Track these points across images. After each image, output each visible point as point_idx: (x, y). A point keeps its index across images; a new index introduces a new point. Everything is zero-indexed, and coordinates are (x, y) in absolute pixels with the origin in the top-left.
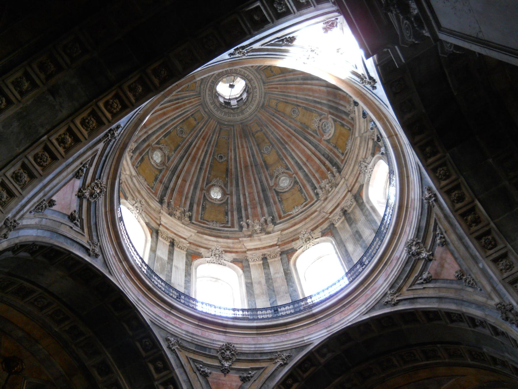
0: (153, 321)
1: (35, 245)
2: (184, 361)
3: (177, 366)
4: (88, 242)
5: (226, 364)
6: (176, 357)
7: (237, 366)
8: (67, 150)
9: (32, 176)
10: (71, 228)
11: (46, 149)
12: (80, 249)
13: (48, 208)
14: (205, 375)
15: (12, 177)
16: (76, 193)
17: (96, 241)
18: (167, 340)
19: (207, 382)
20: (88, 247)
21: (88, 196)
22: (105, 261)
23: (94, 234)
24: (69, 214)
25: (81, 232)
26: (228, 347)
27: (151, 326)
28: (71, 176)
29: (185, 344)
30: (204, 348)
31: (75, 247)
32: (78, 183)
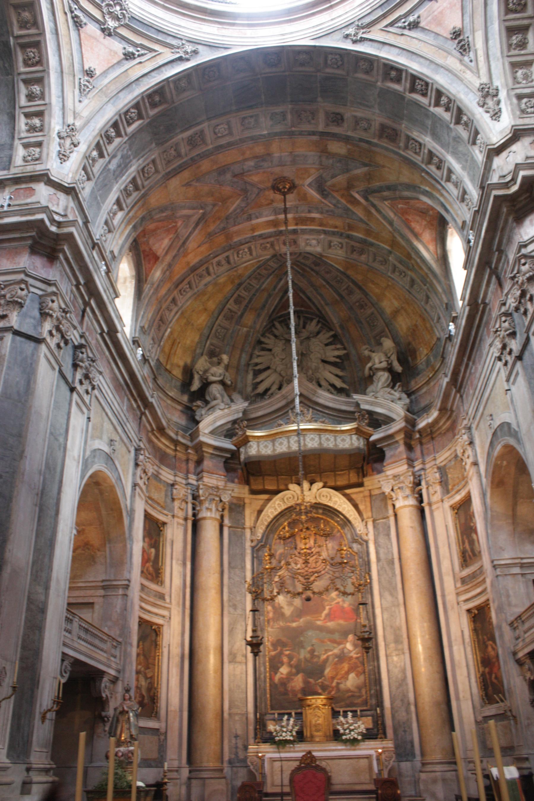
0: (315, 37)
1: (126, 113)
3: (378, 49)
4: (173, 53)
6: (370, 43)
9: (40, 81)
10: (140, 63)
11: (24, 47)
12: (173, 67)
13: (91, 80)
15: (29, 101)
16: (103, 36)
17: (180, 42)
20: (178, 56)
21: (116, 24)
22: (210, 46)
23: (169, 40)
24: (123, 56)
25: (154, 54)
27: (317, 44)
28: (73, 34)
31: (166, 71)
32: (92, 28)
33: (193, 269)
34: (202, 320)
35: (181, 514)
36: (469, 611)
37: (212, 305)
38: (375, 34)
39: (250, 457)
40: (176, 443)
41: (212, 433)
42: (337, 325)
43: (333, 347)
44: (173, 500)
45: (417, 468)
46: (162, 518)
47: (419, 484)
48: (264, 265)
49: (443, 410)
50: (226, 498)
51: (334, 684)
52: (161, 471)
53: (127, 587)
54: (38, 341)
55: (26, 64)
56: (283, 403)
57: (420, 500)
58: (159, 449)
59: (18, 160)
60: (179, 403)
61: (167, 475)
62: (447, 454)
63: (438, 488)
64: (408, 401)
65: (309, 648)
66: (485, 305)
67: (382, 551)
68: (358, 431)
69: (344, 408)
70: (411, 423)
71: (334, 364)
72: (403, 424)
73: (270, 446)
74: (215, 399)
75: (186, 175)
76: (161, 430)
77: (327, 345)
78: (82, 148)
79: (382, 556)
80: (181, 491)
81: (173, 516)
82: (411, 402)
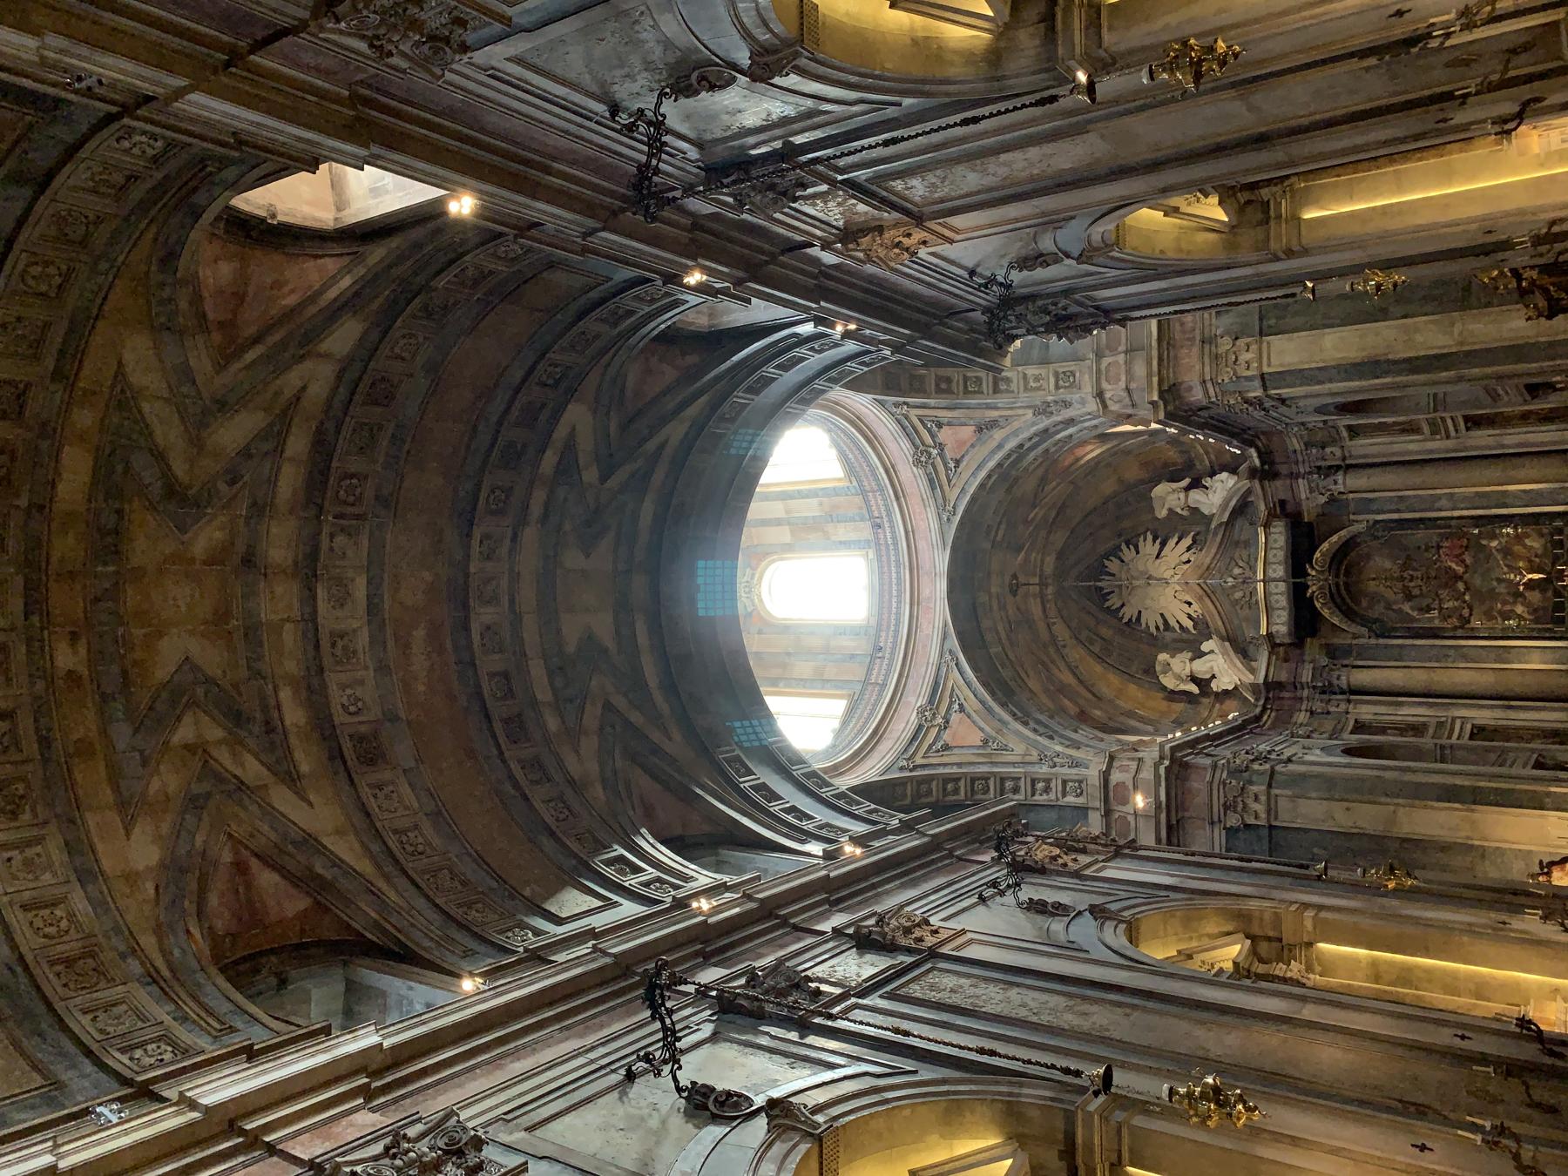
2: (957, 491)
5: (935, 452)
7: (929, 440)
8: (955, 779)
9: (1003, 780)
14: (957, 462)
18: (948, 519)
19: (963, 456)
26: (917, 463)
28: (956, 751)
29: (940, 501)
30: (931, 481)
32: (947, 736)
33: (1081, 682)
34: (1114, 679)
35: (1343, 706)
36: (1468, 429)
37: (1099, 669)
38: (952, 495)
39: (1290, 634)
40: (1264, 709)
41: (1253, 671)
42: (1117, 542)
43: (1141, 544)
44: (1328, 713)
45: (1302, 470)
46: (1352, 723)
47: (1319, 468)
48: (1059, 611)
49: (1251, 444)
50: (1324, 661)
51: (1537, 560)
52: (1299, 721)
53: (1442, 747)
54: (1273, 772)
55: (986, 791)
56: (1207, 600)
57: (1338, 468)
58: (1273, 723)
59: (1081, 801)
60: (1213, 706)
61: (1302, 717)
62: (1295, 441)
63: (1328, 450)
64: (1224, 475)
65: (1495, 583)
66: (1212, 418)
67: (1386, 508)
68: (1266, 526)
69: (1219, 539)
70: (1253, 473)
71: (1163, 544)
72: (1257, 483)
73: (1279, 612)
74: (1212, 668)
75: (1023, 675)
76: (1258, 718)
77: (1138, 552)
78: (1059, 748)
79: (1393, 507)
80: (1318, 706)
81: (1347, 713)
82: (1221, 471)
